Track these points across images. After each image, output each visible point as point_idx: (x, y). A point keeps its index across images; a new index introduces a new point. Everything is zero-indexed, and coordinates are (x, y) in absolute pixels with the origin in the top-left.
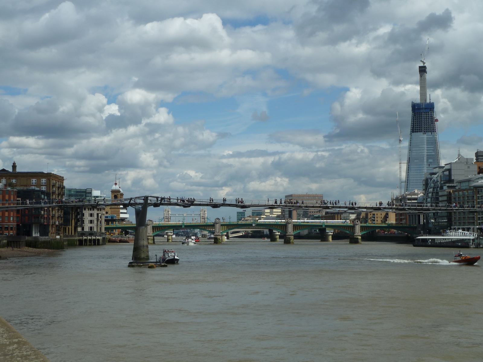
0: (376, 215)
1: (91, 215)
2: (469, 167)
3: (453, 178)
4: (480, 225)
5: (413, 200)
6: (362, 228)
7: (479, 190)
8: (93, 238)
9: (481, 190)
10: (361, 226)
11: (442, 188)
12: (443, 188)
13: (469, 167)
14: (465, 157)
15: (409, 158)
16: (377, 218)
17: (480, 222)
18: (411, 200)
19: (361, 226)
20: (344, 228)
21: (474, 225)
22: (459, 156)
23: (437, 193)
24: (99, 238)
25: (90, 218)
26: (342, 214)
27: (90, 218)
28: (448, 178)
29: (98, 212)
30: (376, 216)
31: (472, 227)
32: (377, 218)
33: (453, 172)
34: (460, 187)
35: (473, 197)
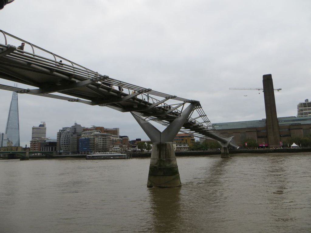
3: (77, 132)
6: (30, 153)
11: (72, 135)
15: (7, 128)
30: (12, 149)
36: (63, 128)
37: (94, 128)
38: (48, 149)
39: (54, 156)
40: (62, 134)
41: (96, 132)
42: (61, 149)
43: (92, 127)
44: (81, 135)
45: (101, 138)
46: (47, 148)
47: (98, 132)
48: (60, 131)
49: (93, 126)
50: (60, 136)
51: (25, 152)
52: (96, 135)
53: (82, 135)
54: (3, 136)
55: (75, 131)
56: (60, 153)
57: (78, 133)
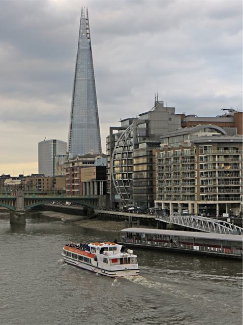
0: (42, 180)
2: (170, 119)
3: (152, 132)
4: (203, 199)
5: (89, 163)
7: (202, 147)
9: (205, 147)
10: (25, 199)
11: (137, 146)
12: (138, 147)
13: (170, 119)
15: (71, 125)
16: (43, 184)
17: (203, 196)
18: (86, 163)
19: (25, 199)
20: (3, 201)
21: (194, 200)
22: (156, 106)
26: (5, 179)
28: (144, 133)
30: (42, 182)
31: (190, 203)
32: (43, 184)
33: (152, 125)
34: (167, 144)
35: (193, 157)
36: (122, 121)
37: (228, 116)
38: (96, 186)
39: (97, 211)
40: (116, 141)
41: (204, 134)
42: (114, 193)
43: (222, 113)
44: (158, 144)
45: (214, 156)
46: (93, 182)
48: (111, 132)
49: (231, 111)
50: (112, 149)
51: (15, 200)
52: (197, 144)
54: (55, 146)
56: (116, 206)
57: (153, 136)
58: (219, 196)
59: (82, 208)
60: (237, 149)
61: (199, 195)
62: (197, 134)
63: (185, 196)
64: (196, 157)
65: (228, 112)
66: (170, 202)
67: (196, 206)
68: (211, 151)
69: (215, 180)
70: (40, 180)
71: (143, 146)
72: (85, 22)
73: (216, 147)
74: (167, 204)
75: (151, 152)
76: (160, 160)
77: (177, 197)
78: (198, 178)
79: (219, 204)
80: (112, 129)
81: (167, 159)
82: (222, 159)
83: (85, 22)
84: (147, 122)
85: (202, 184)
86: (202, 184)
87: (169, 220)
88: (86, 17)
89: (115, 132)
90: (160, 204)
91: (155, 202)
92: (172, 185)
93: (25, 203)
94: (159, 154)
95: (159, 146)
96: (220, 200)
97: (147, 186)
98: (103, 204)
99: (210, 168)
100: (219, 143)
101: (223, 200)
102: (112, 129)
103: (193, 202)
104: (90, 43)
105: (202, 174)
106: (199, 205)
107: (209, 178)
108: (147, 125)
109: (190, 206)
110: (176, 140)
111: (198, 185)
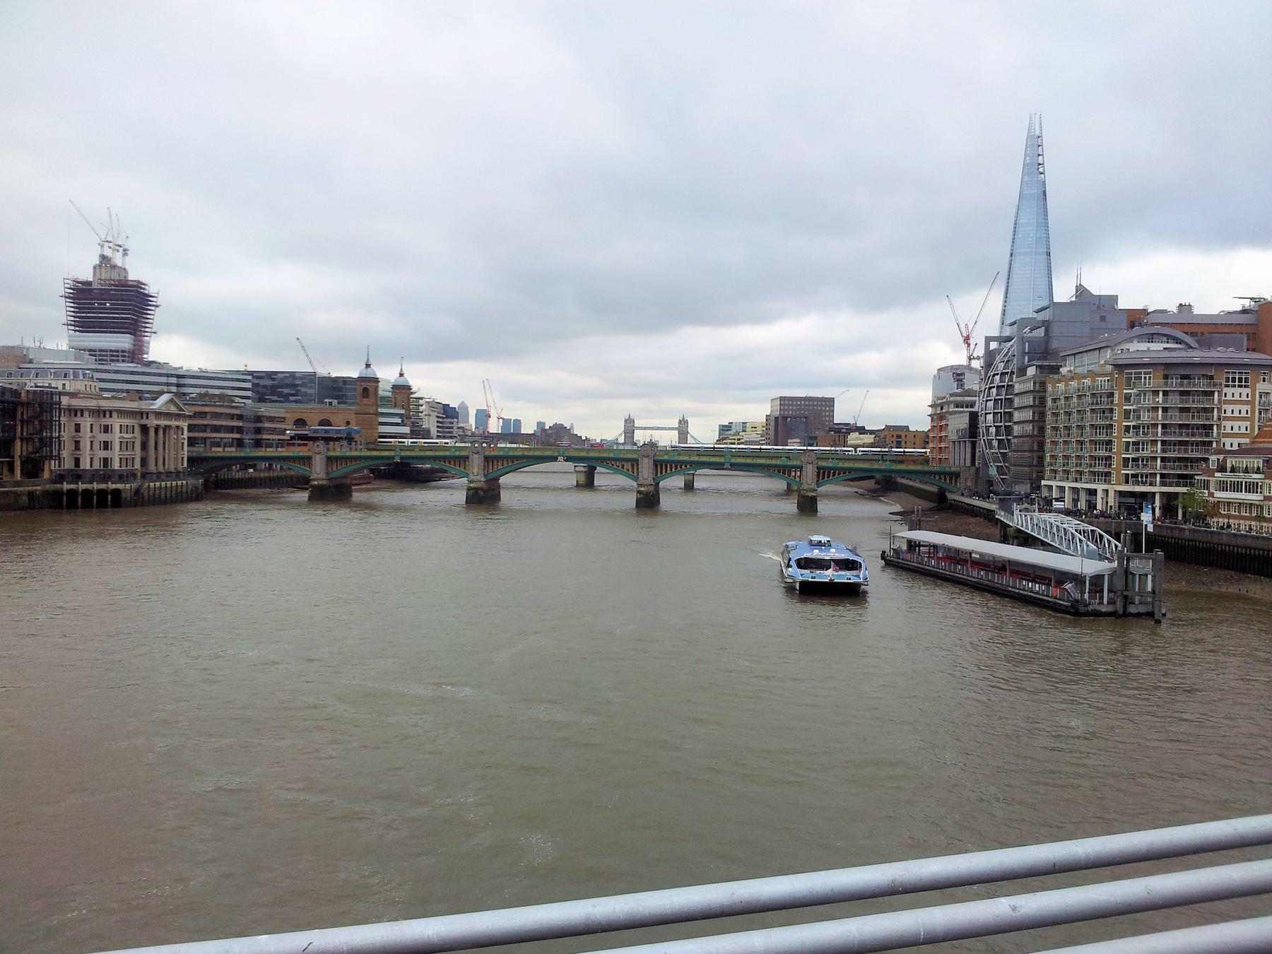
1: (106, 429)
2: (1103, 319)
4: (1127, 482)
8: (96, 486)
11: (1022, 371)
13: (1103, 319)
14: (1095, 292)
21: (1109, 483)
23: (1010, 387)
24: (119, 486)
25: (104, 437)
27: (104, 437)
29: (144, 422)
31: (1100, 487)
33: (1055, 331)
35: (1112, 395)
37: (1244, 311)
41: (1143, 346)
43: (1237, 306)
44: (1055, 370)
47: (1157, 346)
53: (1064, 370)
55: (1047, 342)
58: (1162, 476)
59: (934, 489)
60: (1211, 378)
61: (1118, 473)
62: (1125, 346)
63: (1094, 473)
64: (1116, 396)
65: (1247, 303)
66: (1067, 485)
67: (1111, 494)
68: (1152, 381)
69: (1154, 442)
70: (899, 436)
71: (1031, 371)
72: (1035, 144)
73: (1161, 373)
74: (1062, 489)
75: (1043, 384)
76: (1054, 400)
77: (1079, 476)
78: (1119, 438)
79: (1162, 494)
80: (988, 340)
81: (1079, 396)
82: (1175, 401)
83: (1035, 144)
84: (1047, 325)
85: (1127, 450)
86: (1127, 450)
87: (1012, 520)
88: (1037, 133)
89: (993, 345)
90: (1050, 488)
91: (1043, 482)
92: (1073, 451)
93: (818, 476)
94: (1054, 386)
95: (1058, 373)
96: (1163, 484)
97: (1030, 451)
98: (969, 483)
99: (1146, 418)
100: (1166, 364)
101: (1178, 485)
102: (988, 340)
103: (1106, 487)
104: (1044, 183)
105: (1127, 429)
106: (1121, 494)
107: (1141, 438)
108: (1047, 331)
109: (1100, 494)
110: (1086, 358)
111: (1118, 453)
